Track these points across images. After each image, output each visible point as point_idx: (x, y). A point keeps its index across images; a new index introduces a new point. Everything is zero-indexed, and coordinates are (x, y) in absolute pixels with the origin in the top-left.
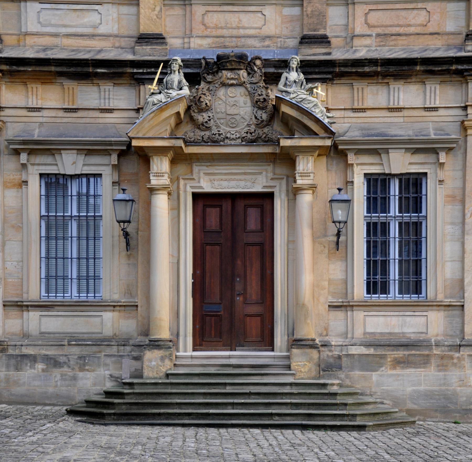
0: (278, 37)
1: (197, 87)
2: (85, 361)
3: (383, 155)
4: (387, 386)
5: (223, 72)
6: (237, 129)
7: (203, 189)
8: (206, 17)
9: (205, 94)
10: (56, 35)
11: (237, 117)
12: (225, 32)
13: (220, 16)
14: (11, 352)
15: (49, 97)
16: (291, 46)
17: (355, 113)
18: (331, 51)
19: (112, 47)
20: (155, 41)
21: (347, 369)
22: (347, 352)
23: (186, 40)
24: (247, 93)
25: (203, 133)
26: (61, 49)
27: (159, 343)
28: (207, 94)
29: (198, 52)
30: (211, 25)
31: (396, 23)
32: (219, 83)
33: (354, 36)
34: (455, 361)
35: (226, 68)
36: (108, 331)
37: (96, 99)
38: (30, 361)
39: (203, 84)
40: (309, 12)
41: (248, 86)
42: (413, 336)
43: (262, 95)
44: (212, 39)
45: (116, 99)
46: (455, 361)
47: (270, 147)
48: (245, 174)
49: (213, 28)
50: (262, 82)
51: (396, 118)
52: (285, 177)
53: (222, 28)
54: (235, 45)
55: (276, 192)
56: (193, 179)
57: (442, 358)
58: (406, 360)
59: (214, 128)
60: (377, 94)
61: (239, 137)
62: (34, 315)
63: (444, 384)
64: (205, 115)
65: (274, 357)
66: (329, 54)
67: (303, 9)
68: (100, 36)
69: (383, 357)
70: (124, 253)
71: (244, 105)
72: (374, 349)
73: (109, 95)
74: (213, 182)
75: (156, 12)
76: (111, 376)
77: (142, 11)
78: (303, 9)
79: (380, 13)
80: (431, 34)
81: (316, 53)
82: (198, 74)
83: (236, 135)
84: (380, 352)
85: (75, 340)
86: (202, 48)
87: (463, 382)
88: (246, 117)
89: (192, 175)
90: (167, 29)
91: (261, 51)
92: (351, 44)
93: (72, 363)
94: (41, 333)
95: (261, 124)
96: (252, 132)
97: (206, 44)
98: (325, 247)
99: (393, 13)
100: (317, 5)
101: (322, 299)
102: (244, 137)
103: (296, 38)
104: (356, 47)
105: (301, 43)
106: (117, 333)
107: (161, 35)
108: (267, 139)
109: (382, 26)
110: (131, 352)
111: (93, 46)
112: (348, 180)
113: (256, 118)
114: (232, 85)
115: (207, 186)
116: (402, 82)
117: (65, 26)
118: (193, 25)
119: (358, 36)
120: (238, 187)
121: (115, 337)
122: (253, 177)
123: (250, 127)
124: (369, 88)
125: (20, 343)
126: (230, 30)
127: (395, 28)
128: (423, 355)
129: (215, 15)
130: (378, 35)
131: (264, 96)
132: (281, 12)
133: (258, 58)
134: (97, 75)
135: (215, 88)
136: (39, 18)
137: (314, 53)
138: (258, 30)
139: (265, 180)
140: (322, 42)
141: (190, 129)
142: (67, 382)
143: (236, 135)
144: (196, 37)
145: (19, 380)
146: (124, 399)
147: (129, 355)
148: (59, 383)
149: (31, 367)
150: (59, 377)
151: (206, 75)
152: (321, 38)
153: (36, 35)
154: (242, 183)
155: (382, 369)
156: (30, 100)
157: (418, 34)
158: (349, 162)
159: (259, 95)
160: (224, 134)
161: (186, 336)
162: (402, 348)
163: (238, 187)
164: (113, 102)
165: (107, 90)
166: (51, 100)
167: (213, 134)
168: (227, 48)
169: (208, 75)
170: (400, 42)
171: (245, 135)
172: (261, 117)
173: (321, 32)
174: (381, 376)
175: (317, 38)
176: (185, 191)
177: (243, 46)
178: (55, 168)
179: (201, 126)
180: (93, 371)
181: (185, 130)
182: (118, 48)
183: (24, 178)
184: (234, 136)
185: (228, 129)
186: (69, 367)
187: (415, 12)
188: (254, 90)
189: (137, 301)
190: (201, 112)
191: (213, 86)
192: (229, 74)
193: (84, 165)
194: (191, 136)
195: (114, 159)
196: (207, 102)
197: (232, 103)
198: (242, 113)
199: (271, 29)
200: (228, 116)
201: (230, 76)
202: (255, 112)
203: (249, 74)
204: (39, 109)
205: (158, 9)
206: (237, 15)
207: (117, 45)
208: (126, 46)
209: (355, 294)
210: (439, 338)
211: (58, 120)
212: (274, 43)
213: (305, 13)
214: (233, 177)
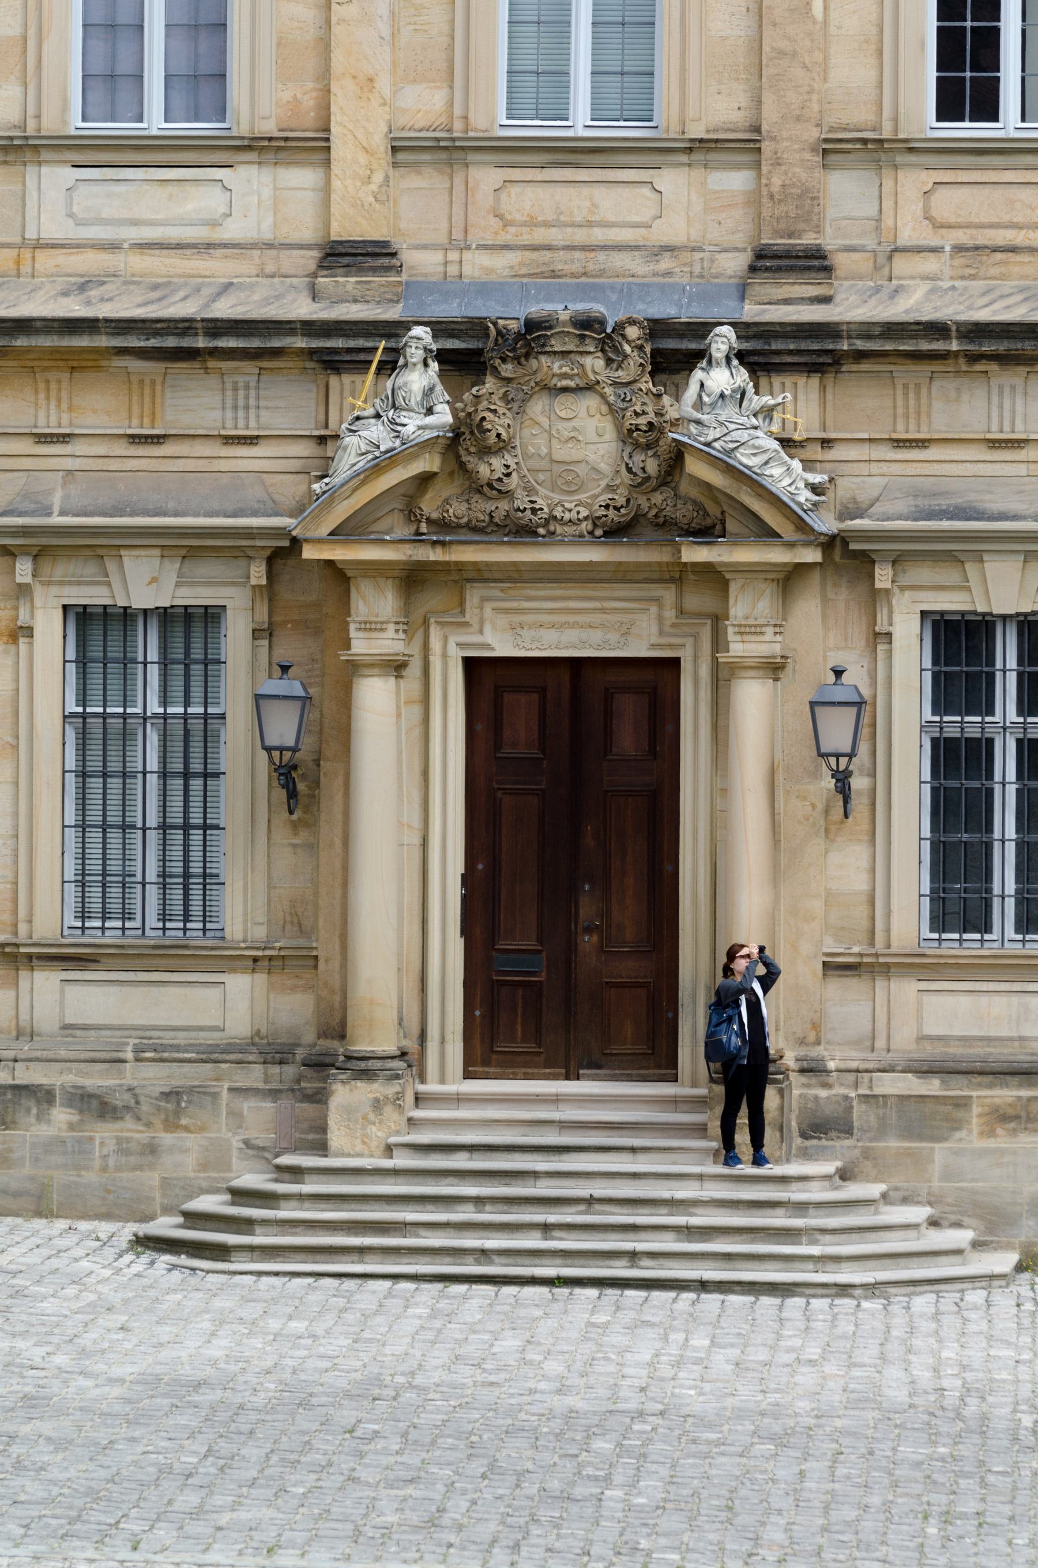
0: (694, 250)
1: (474, 391)
2: (178, 1104)
3: (968, 566)
4: (973, 1180)
5: (543, 359)
6: (582, 496)
7: (493, 649)
8: (504, 196)
9: (495, 411)
10: (113, 247)
11: (581, 470)
12: (555, 236)
13: (540, 191)
15: (98, 409)
16: (730, 272)
17: (898, 450)
18: (832, 292)
19: (258, 276)
20: (370, 262)
21: (868, 1135)
22: (871, 1088)
23: (453, 256)
24: (604, 408)
25: (490, 506)
26: (126, 283)
27: (372, 1064)
28: (501, 411)
29: (484, 289)
30: (518, 217)
31: (1006, 218)
32: (533, 384)
33: (896, 250)
35: (548, 349)
36: (239, 1024)
37: (213, 409)
38: (38, 1102)
39: (490, 383)
40: (775, 188)
41: (608, 390)
43: (644, 413)
44: (519, 253)
45: (267, 408)
47: (664, 549)
48: (603, 610)
49: (524, 224)
50: (647, 377)
51: (1008, 466)
52: (709, 622)
53: (546, 224)
54: (581, 270)
55: (686, 657)
56: (466, 624)
58: (1023, 1114)
59: (520, 493)
60: (958, 399)
61: (586, 518)
62: (45, 984)
64: (497, 462)
65: (674, 1103)
66: (826, 300)
67: (759, 175)
68: (225, 246)
71: (596, 439)
72: (943, 1082)
73: (247, 397)
74: (519, 631)
75: (374, 187)
76: (247, 1143)
77: (336, 183)
78: (759, 175)
79: (965, 190)
81: (785, 304)
82: (479, 352)
83: (578, 513)
84: (959, 1088)
85: (155, 1049)
86: (493, 278)
88: (603, 466)
89: (463, 612)
90: (403, 225)
91: (648, 285)
92: (886, 271)
93: (145, 1108)
94: (65, 1027)
95: (641, 484)
96: (619, 505)
97: (504, 268)
98: (813, 806)
99: (999, 193)
100: (798, 170)
101: (806, 947)
102: (599, 518)
103: (744, 250)
104: (900, 278)
105: (753, 269)
106: (264, 1031)
107: (385, 244)
108: (661, 520)
109: (969, 226)
110: (298, 1081)
111: (207, 273)
112: (877, 629)
113: (629, 470)
114: (565, 390)
115: (502, 645)
116: (1022, 370)
117: (136, 223)
118: (471, 217)
119: (905, 250)
120: (584, 644)
121: (257, 1040)
122: (625, 618)
123: (614, 491)
124: (936, 384)
125: (11, 1054)
126: (569, 230)
127: (1002, 232)
129: (529, 191)
130: (959, 249)
131: (651, 417)
132: (704, 184)
133: (632, 322)
135: (521, 395)
136: (70, 203)
137: (787, 296)
138: (642, 231)
139: (654, 629)
140: (809, 268)
141: (458, 491)
142: (133, 1160)
143: (578, 513)
144: (480, 247)
145: (11, 1151)
146: (278, 1209)
147: (293, 1090)
148: (111, 1162)
149: (38, 1118)
150: (111, 1146)
151: (498, 362)
152: (807, 257)
153: (62, 246)
154: (596, 636)
155: (958, 1135)
156: (42, 414)
158: (878, 585)
159: (637, 414)
160: (546, 510)
161: (443, 1041)
162: (1017, 1079)
163: (584, 644)
164: (258, 416)
165: (241, 385)
166: (95, 412)
167: (518, 509)
168: (559, 277)
169: (504, 360)
170: (1016, 269)
171: (602, 512)
172: (643, 469)
173: (808, 240)
174: (957, 1153)
175: (797, 257)
176: (445, 656)
177: (602, 273)
178: (103, 590)
179: (486, 489)
180: (202, 1129)
181: (445, 494)
182: (273, 276)
183: (23, 618)
184: (573, 515)
185: (557, 497)
186: (139, 1119)
188: (623, 400)
189: (314, 945)
190: (486, 453)
191: (517, 390)
192: (558, 366)
193: (178, 585)
194: (459, 513)
195: (258, 574)
196: (501, 431)
197: (567, 434)
198: (592, 457)
199: (673, 229)
200: (555, 465)
201: (561, 367)
202: (626, 455)
203: (609, 361)
204: (64, 438)
205: (378, 177)
206: (585, 190)
207: (270, 268)
208: (293, 272)
209: (894, 934)
211: (114, 464)
212: (685, 265)
213: (765, 192)
214: (571, 618)
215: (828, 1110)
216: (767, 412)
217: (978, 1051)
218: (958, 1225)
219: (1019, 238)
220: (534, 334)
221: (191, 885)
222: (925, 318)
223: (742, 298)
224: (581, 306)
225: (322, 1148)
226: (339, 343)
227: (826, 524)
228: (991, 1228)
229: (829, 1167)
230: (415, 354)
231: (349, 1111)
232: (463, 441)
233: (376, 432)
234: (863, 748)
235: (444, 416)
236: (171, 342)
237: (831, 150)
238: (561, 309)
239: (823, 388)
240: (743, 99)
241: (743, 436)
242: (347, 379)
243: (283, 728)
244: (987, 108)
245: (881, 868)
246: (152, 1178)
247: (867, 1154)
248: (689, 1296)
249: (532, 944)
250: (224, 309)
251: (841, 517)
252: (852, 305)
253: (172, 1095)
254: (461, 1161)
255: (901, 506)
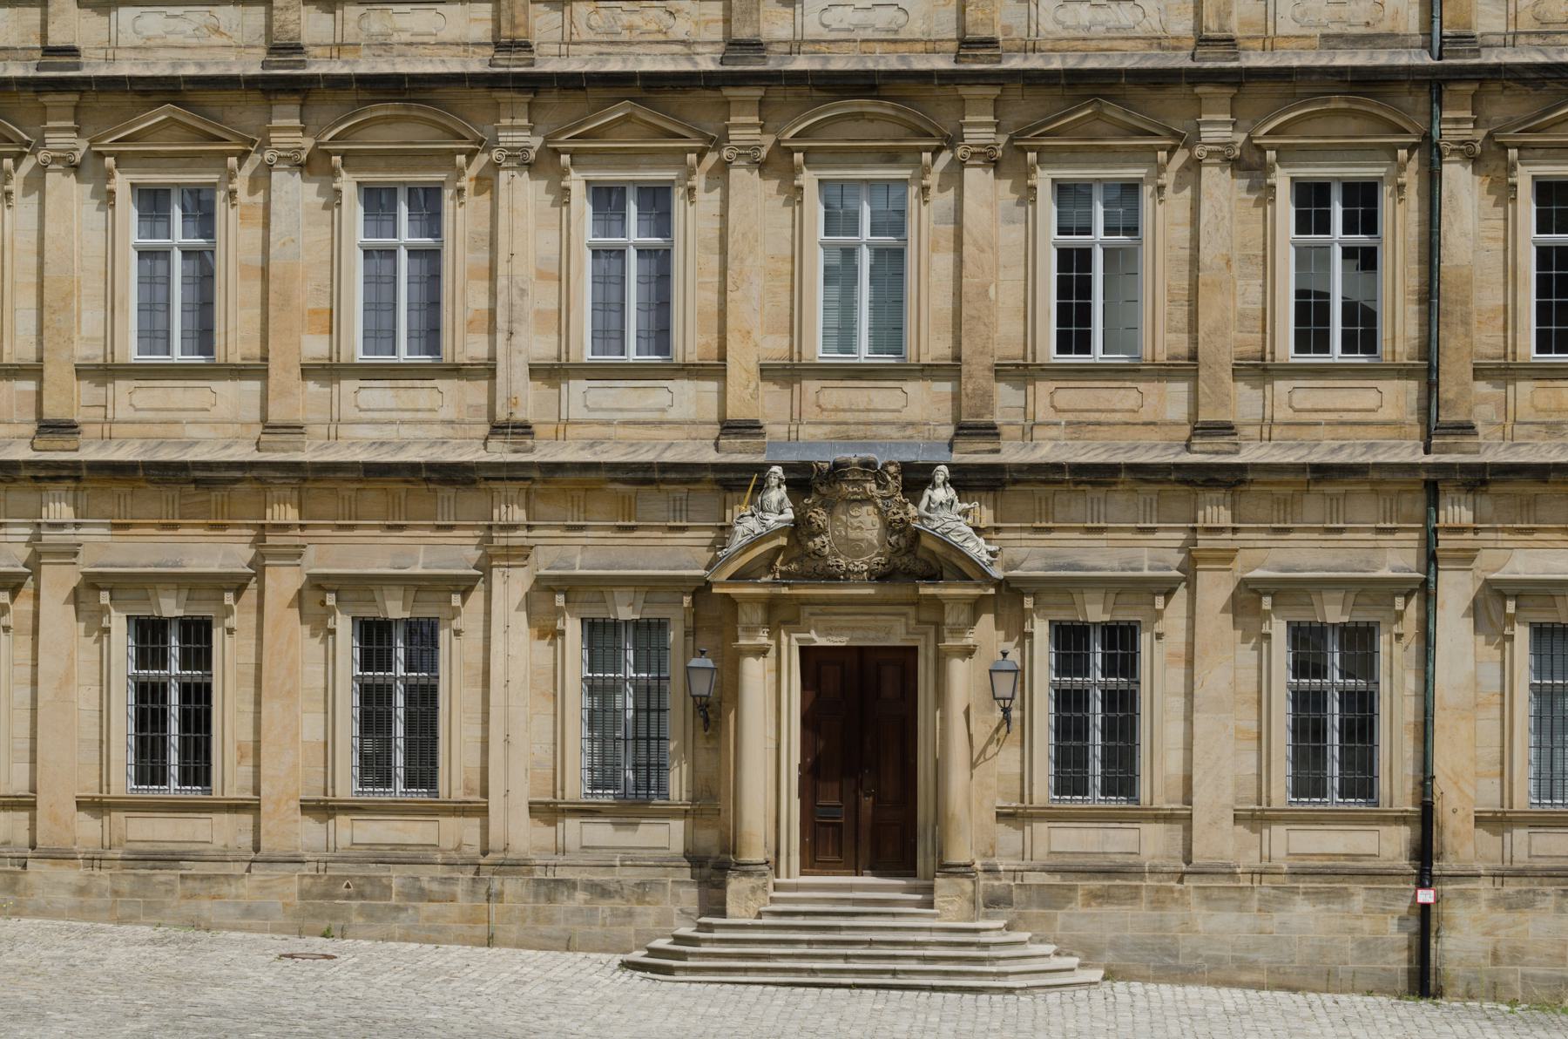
10: (608, 423)
12: (849, 417)
13: (841, 392)
14: (539, 874)
29: (810, 445)
31: (1095, 407)
34: (1176, 895)
42: (1119, 859)
46: (1176, 895)
53: (844, 410)
57: (1158, 890)
63: (1160, 929)
64: (817, 540)
66: (997, 451)
69: (1072, 889)
70: (701, 732)
77: (730, 389)
80: (1145, 424)
81: (974, 454)
82: (808, 480)
85: (631, 859)
87: (1187, 926)
95: (896, 550)
105: (957, 435)
115: (821, 641)
117: (621, 410)
128: (1131, 887)
130: (1069, 424)
131: (902, 515)
133: (891, 463)
134: (663, 481)
150: (608, 912)
157: (1127, 424)
163: (865, 639)
173: (987, 419)
174: (1070, 915)
176: (789, 645)
177: (875, 437)
187: (1122, 392)
199: (914, 413)
203: (879, 486)
205: (753, 385)
206: (866, 392)
207: (694, 435)
210: (1156, 861)
215: (999, 892)
216: (965, 514)
217: (1081, 860)
218: (1070, 955)
219: (1102, 417)
220: (838, 471)
221: (652, 772)
222: (1051, 461)
223: (951, 451)
224: (864, 455)
225: (723, 914)
226: (732, 475)
227: (997, 573)
228: (1088, 957)
229: (1001, 923)
230: (774, 482)
231: (738, 893)
232: (800, 529)
233: (752, 524)
234: (1018, 695)
235: (789, 515)
236: (640, 475)
237: (1001, 372)
238: (852, 456)
239: (995, 500)
240: (950, 342)
241: (953, 525)
242: (736, 495)
243: (702, 687)
244: (1084, 346)
245: (1027, 761)
246: (631, 930)
247: (1020, 916)
248: (925, 994)
249: (836, 802)
250: (669, 457)
251: (1005, 569)
252: (1011, 453)
253: (641, 885)
254: (799, 921)
255: (1038, 563)
